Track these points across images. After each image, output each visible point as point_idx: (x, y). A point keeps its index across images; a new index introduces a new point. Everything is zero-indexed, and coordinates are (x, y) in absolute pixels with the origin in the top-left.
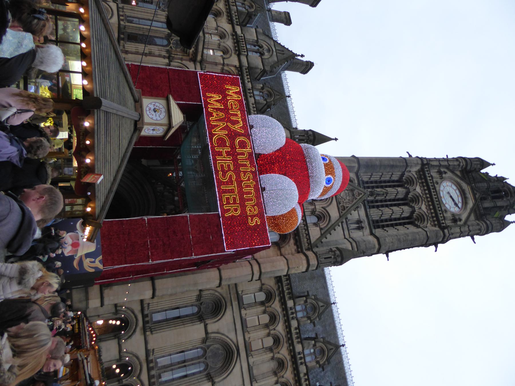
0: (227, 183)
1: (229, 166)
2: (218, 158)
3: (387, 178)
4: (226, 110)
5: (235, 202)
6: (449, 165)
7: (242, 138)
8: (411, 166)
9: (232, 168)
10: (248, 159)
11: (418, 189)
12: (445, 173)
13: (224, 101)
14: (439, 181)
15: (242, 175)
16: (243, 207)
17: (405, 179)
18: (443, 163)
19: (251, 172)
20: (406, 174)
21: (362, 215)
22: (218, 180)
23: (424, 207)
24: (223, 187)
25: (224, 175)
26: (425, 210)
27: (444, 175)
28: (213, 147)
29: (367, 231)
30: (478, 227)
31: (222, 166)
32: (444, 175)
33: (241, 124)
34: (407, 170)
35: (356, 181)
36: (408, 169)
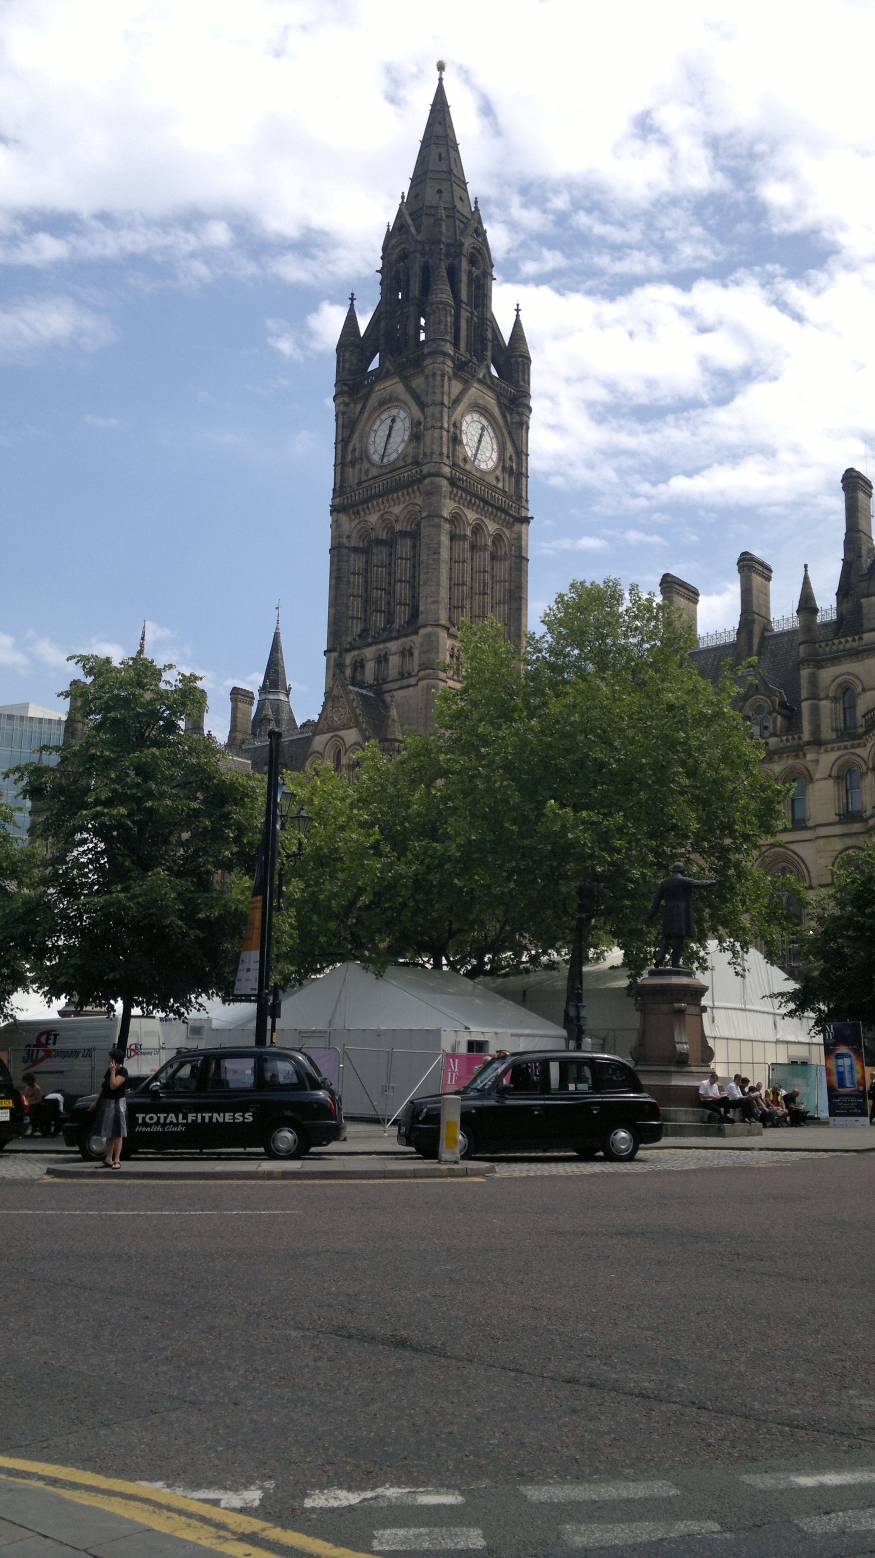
3: (360, 579)
6: (342, 441)
8: (340, 536)
11: (373, 518)
14: (366, 465)
17: (363, 541)
18: (339, 461)
20: (354, 543)
21: (395, 647)
23: (397, 510)
26: (402, 506)
27: (357, 454)
29: (414, 638)
30: (430, 379)
34: (347, 545)
35: (356, 652)
36: (345, 541)
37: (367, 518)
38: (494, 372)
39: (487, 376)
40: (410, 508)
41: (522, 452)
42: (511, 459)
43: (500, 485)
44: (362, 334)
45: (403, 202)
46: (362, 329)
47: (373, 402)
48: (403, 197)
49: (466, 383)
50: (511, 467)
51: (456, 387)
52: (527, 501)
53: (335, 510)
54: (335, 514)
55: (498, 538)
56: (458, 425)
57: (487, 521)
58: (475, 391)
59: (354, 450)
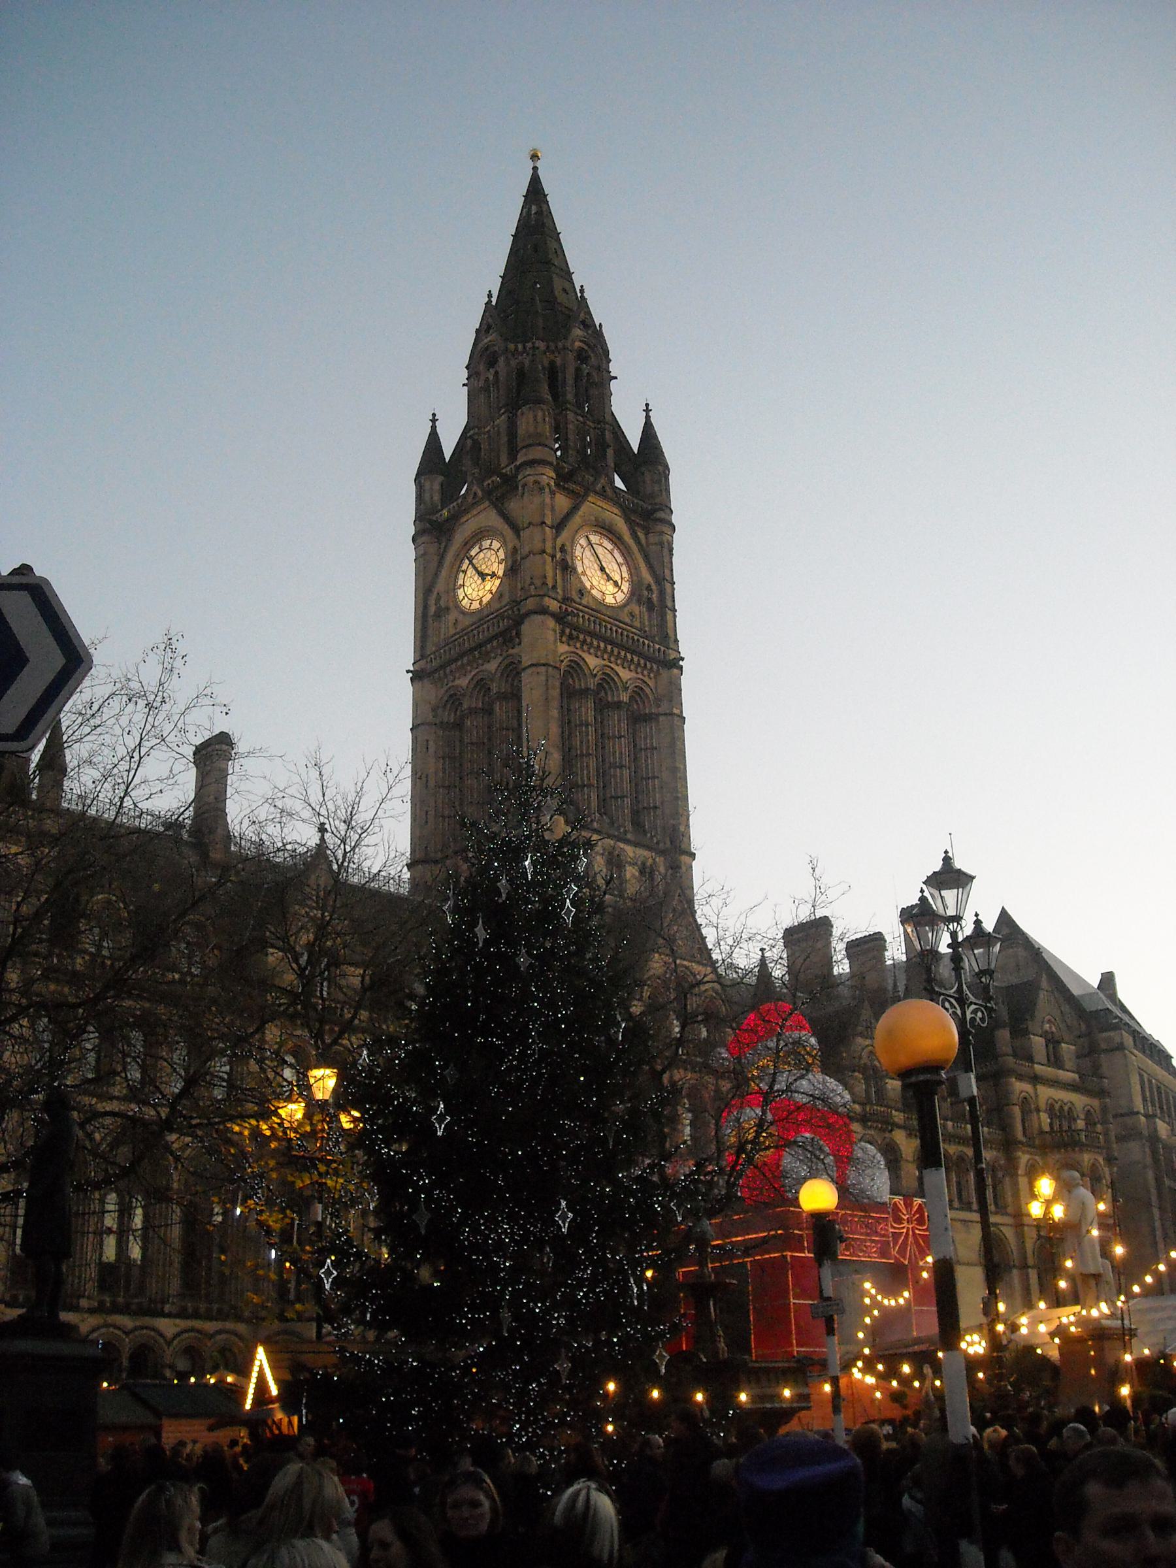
12: (439, 598)
14: (452, 617)
23: (492, 666)
27: (442, 603)
32: (442, 603)
37: (457, 682)
38: (619, 483)
39: (607, 489)
40: (506, 662)
41: (664, 579)
42: (649, 588)
43: (637, 624)
44: (447, 460)
45: (490, 302)
46: (448, 453)
47: (459, 538)
48: (490, 295)
49: (578, 499)
50: (650, 600)
51: (562, 502)
52: (676, 641)
53: (417, 676)
54: (419, 684)
55: (638, 693)
56: (568, 548)
57: (619, 669)
58: (593, 506)
59: (439, 598)
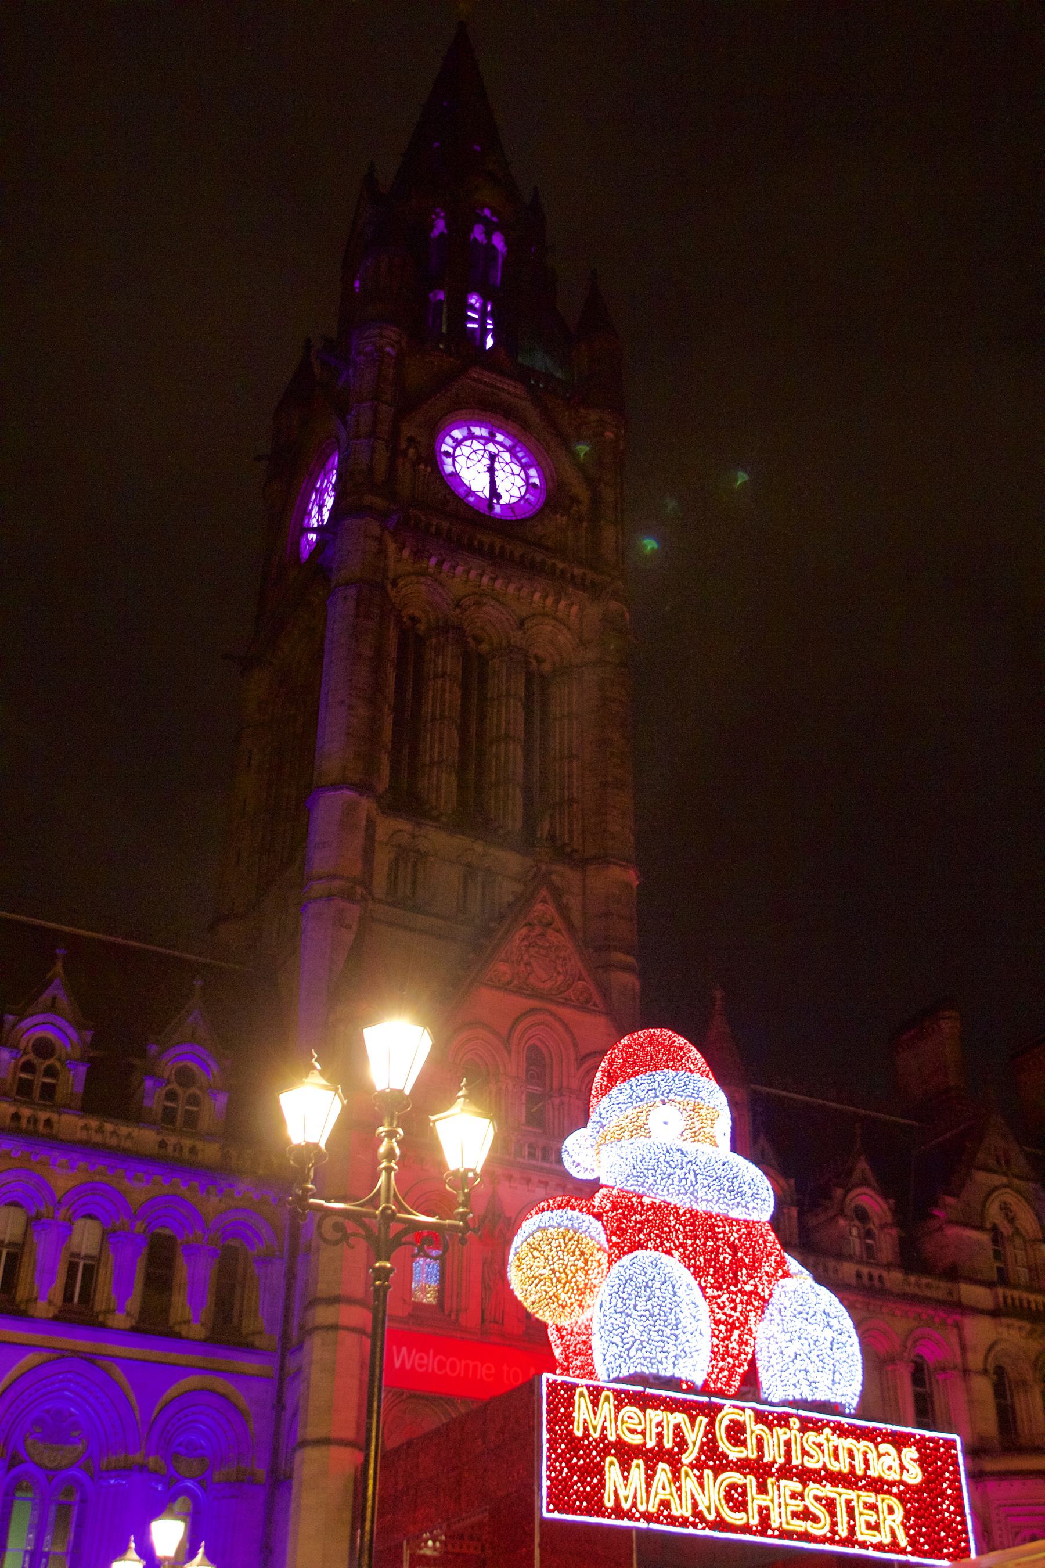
0: (833, 1515)
1: (793, 1496)
2: (775, 1522)
4: (653, 1457)
5: (873, 1507)
7: (721, 1433)
9: (796, 1486)
10: (771, 1431)
13: (626, 1453)
15: (810, 1464)
16: (877, 1485)
19: (803, 1430)
22: (823, 1540)
24: (843, 1532)
25: (816, 1519)
28: (746, 1529)
31: (795, 1515)
33: (680, 1418)
